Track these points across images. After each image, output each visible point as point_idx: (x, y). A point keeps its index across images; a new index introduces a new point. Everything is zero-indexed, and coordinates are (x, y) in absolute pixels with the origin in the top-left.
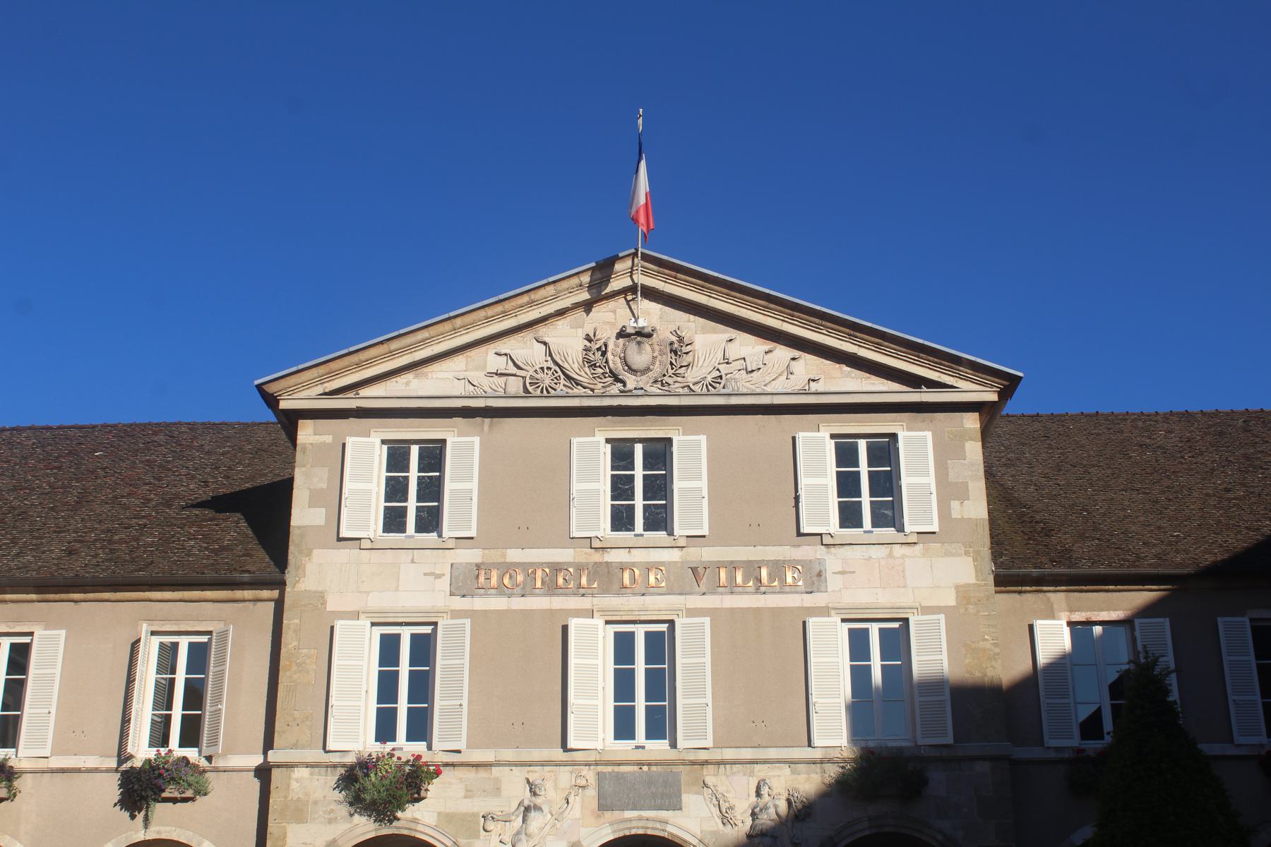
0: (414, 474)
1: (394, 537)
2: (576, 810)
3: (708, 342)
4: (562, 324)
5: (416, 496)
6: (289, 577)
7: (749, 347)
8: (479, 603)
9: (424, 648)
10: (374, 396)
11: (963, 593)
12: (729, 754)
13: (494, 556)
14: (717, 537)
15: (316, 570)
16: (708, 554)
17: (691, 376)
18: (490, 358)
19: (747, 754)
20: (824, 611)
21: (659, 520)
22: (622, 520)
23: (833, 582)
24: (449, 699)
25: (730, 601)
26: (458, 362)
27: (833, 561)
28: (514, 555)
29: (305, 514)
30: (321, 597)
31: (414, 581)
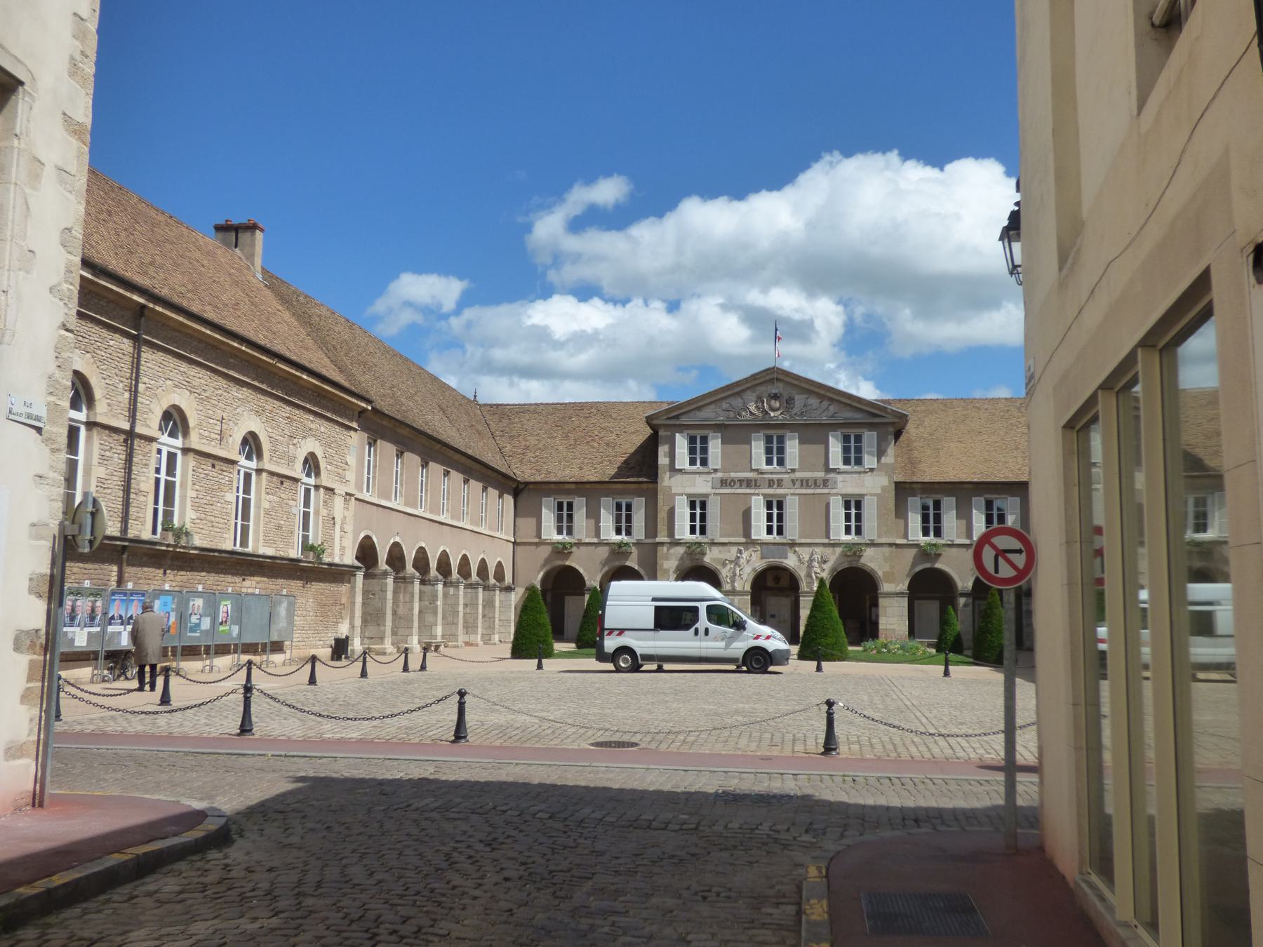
0: (698, 446)
1: (694, 467)
2: (754, 558)
3: (799, 400)
4: (748, 393)
5: (699, 453)
6: (659, 480)
7: (814, 401)
8: (722, 491)
9: (703, 505)
10: (684, 420)
11: (884, 489)
12: (803, 541)
13: (726, 475)
14: (802, 469)
15: (666, 480)
16: (798, 475)
17: (796, 410)
18: (725, 405)
19: (809, 541)
20: (837, 494)
21: (781, 462)
22: (769, 462)
23: (840, 485)
24: (713, 523)
25: (804, 491)
26: (713, 406)
27: (840, 478)
28: (733, 475)
29: (663, 460)
30: (670, 488)
31: (702, 485)
